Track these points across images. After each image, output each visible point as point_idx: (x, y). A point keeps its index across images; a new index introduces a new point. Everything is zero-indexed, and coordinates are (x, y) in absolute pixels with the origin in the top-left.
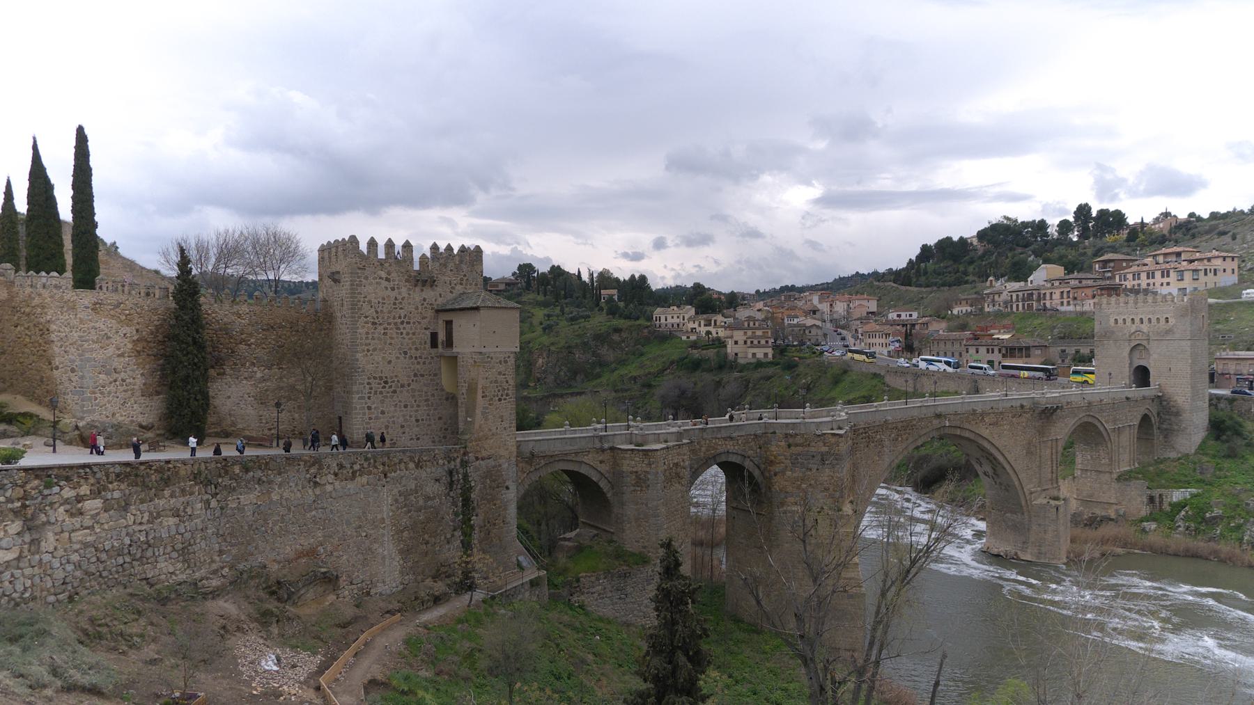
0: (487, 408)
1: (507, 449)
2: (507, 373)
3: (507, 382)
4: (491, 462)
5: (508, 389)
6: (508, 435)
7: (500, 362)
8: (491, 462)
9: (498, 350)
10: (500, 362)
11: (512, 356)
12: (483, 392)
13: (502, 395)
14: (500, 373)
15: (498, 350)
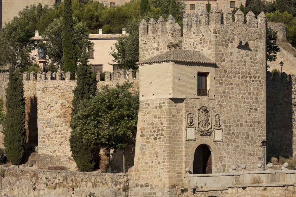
0: (144, 145)
1: (161, 180)
2: (162, 116)
3: (162, 124)
4: (148, 190)
5: (162, 130)
6: (162, 169)
7: (156, 108)
8: (148, 190)
9: (153, 97)
10: (156, 108)
11: (166, 102)
12: (142, 132)
13: (157, 135)
14: (155, 117)
15: (153, 97)
